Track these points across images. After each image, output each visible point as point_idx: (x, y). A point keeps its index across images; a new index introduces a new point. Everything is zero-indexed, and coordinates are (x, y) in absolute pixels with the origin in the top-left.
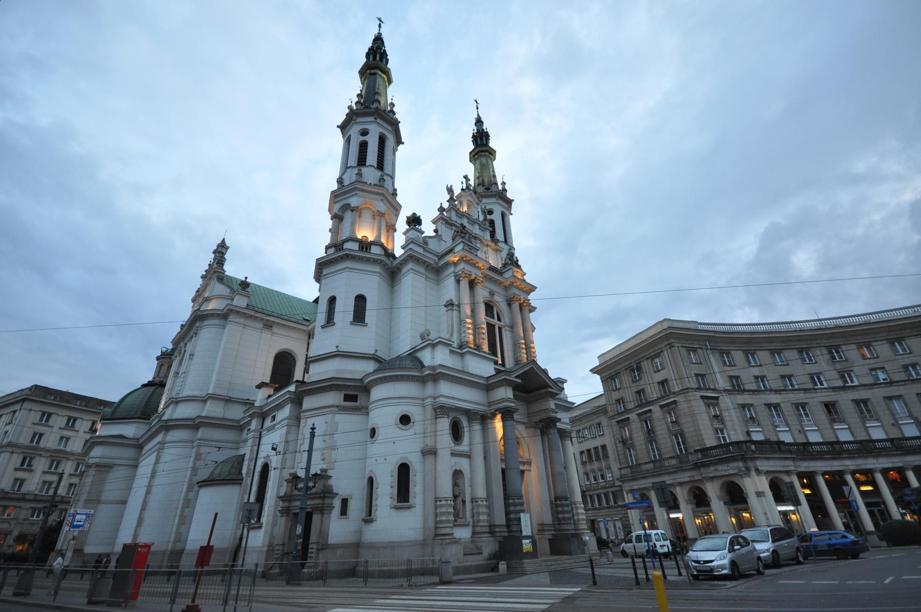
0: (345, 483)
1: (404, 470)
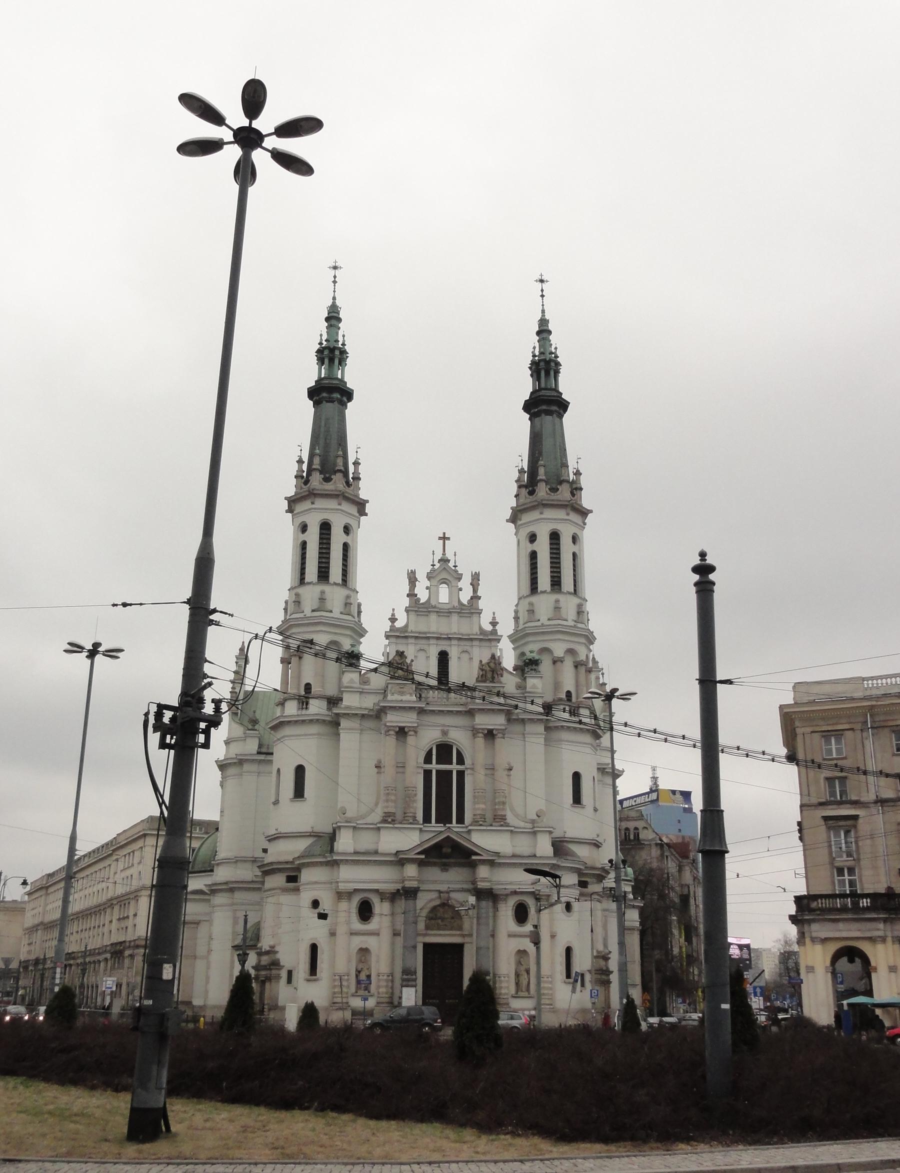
0: (286, 958)
1: (314, 948)
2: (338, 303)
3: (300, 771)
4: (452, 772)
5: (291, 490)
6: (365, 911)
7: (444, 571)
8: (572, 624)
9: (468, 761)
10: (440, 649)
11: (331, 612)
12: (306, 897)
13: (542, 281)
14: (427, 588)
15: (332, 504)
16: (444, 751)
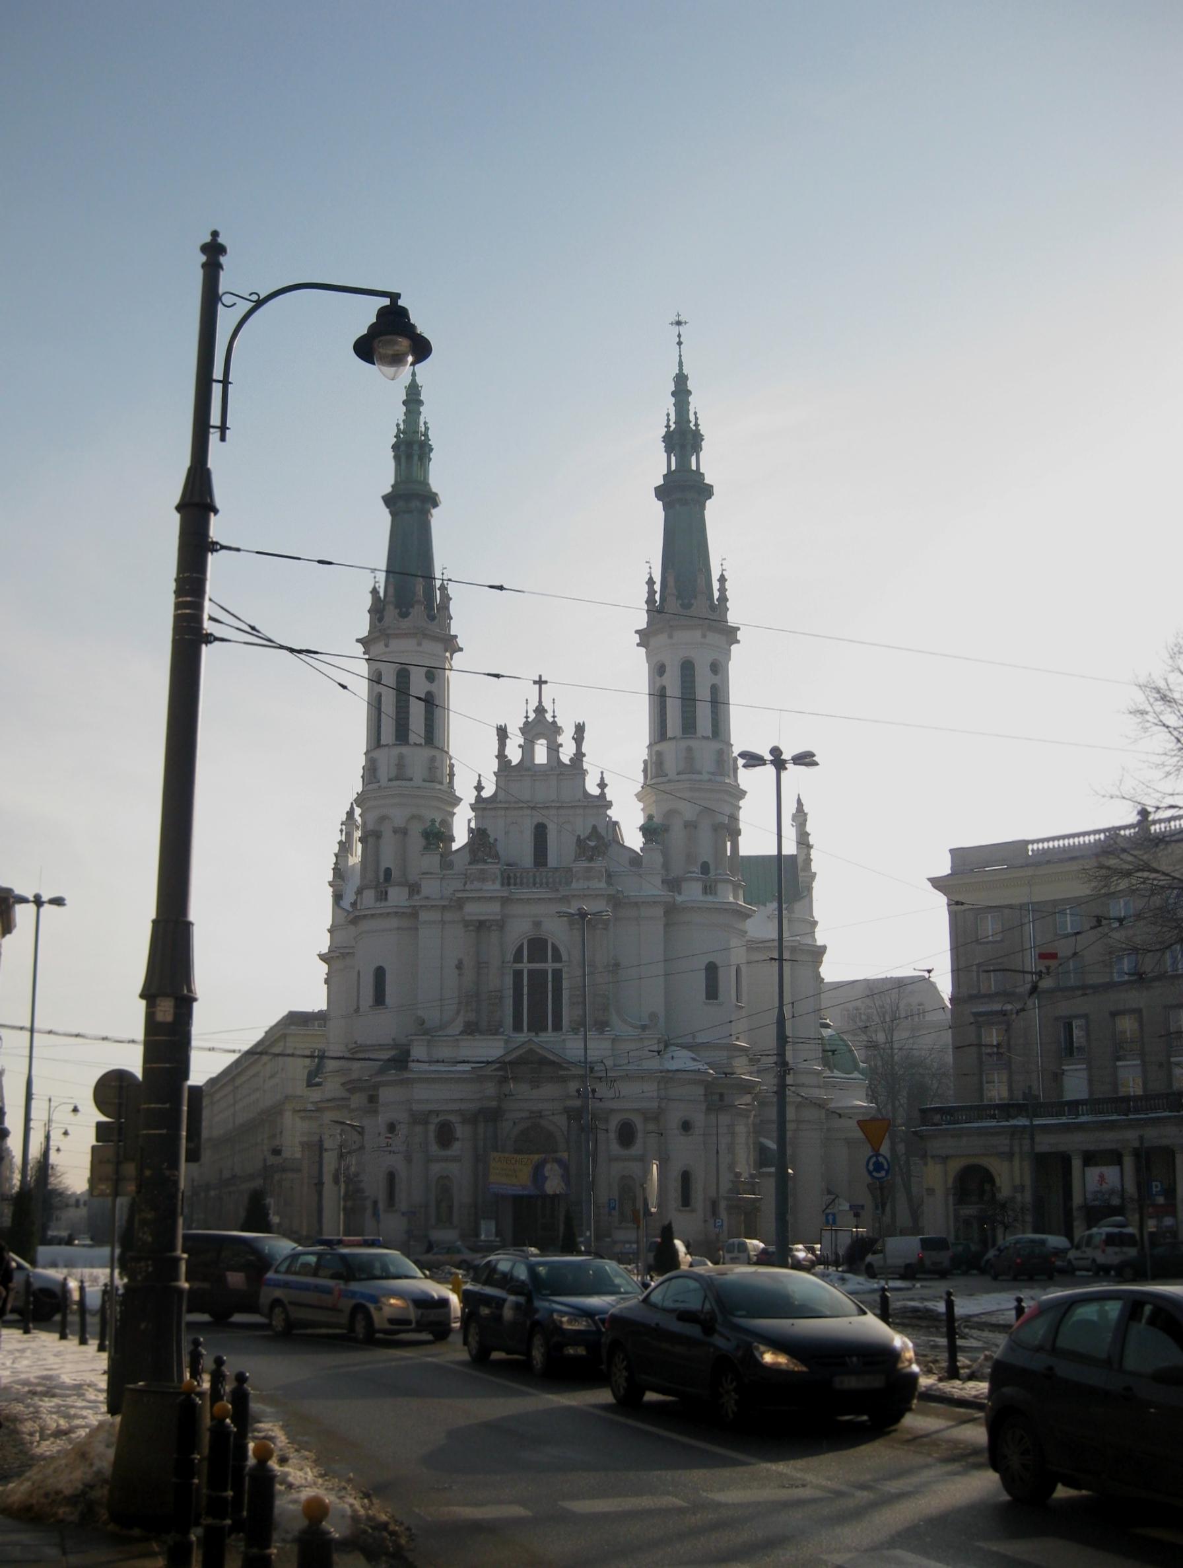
2: (419, 380)
3: (380, 973)
4: (546, 971)
5: (364, 630)
6: (445, 1135)
7: (540, 726)
8: (706, 777)
9: (565, 957)
10: (535, 821)
11: (411, 780)
12: (382, 1120)
13: (679, 323)
14: (520, 746)
15: (409, 644)
16: (538, 947)
